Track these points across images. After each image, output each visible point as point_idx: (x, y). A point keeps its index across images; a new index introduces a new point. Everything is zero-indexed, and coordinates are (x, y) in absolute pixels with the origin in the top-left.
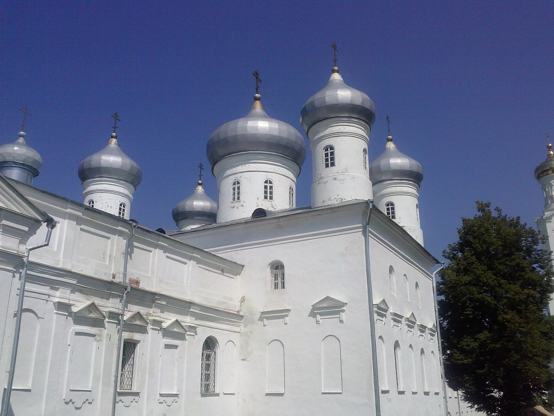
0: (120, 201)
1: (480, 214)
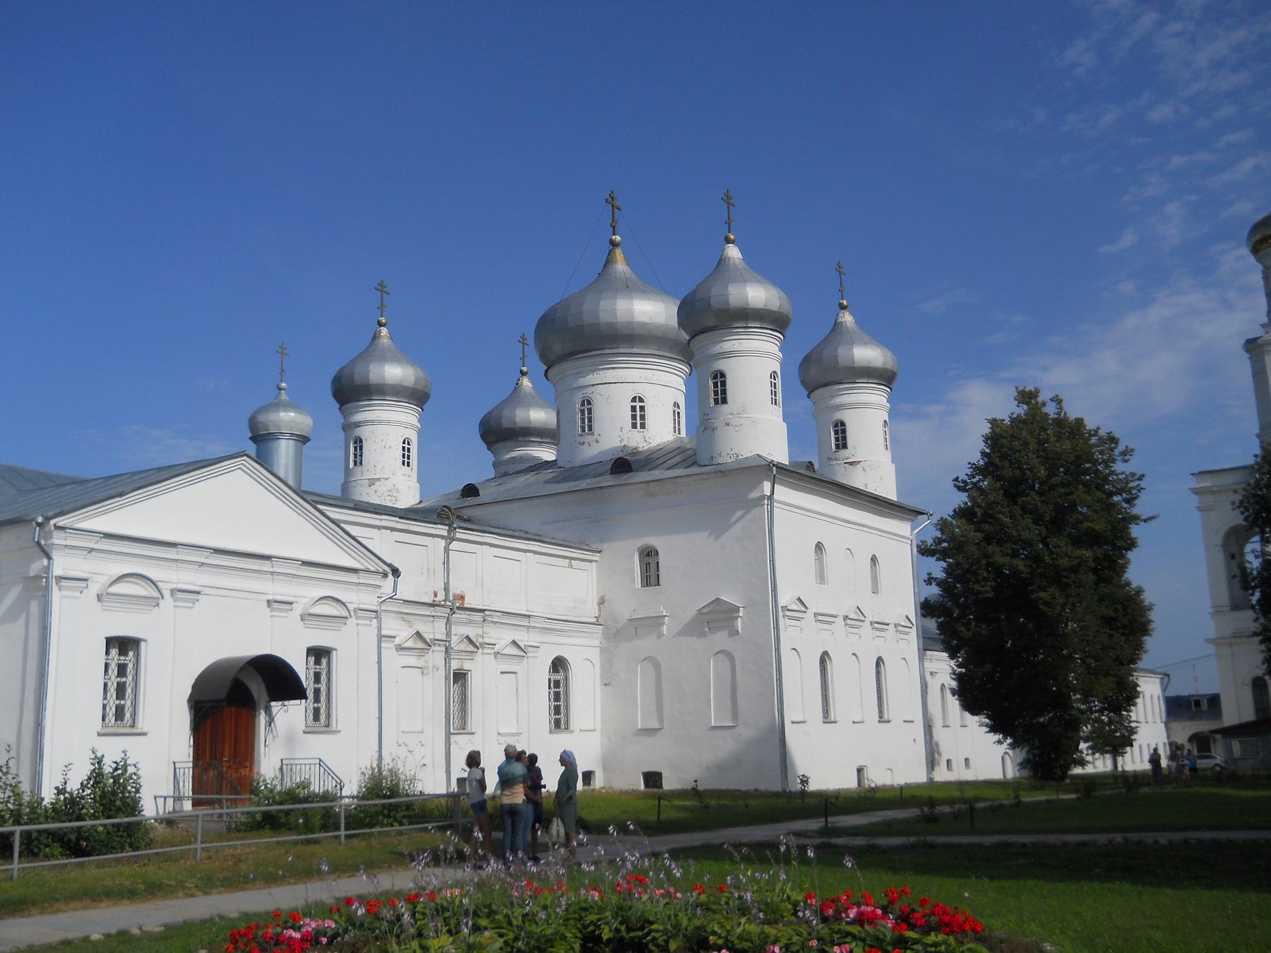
1: (1021, 410)
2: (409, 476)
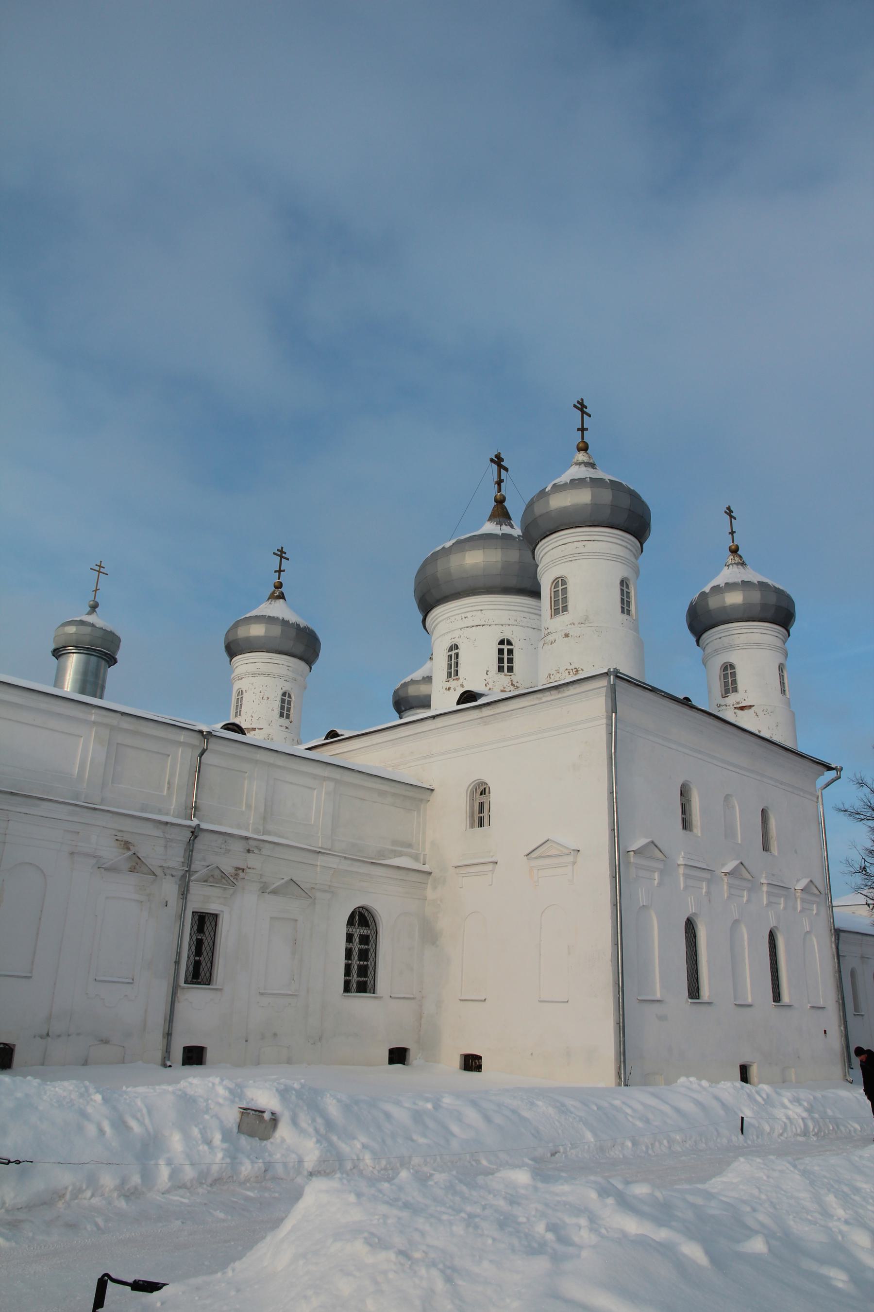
0: (282, 688)
2: (287, 728)
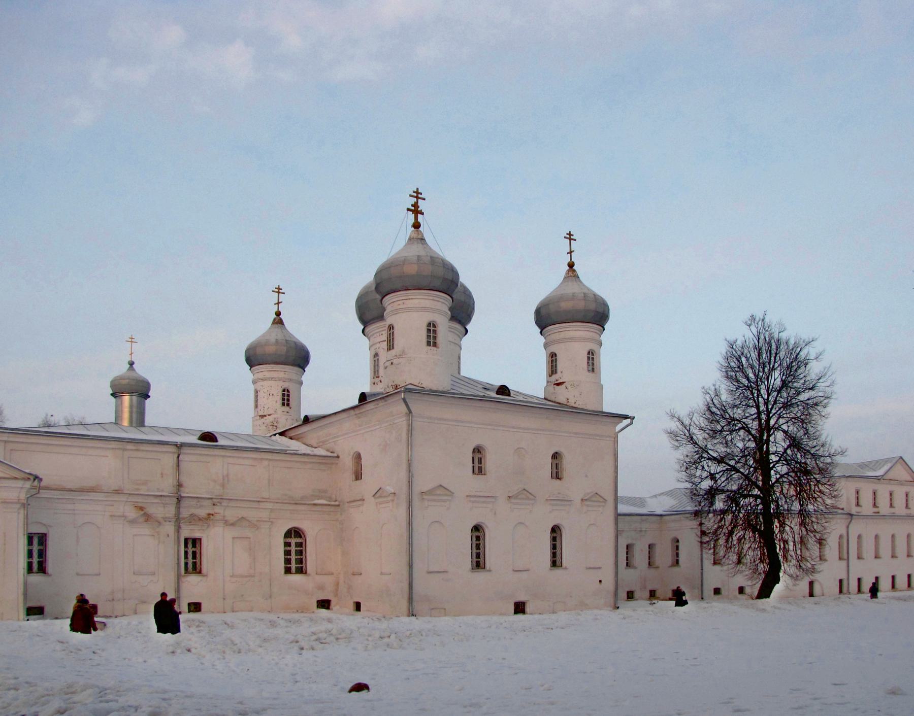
2: (288, 412)
